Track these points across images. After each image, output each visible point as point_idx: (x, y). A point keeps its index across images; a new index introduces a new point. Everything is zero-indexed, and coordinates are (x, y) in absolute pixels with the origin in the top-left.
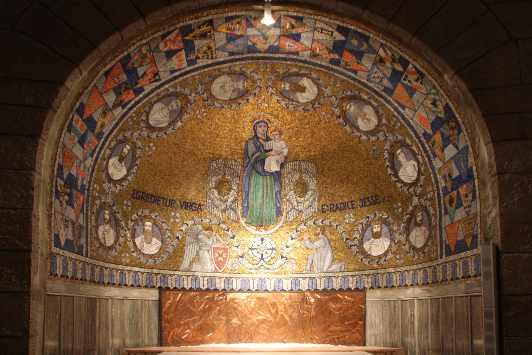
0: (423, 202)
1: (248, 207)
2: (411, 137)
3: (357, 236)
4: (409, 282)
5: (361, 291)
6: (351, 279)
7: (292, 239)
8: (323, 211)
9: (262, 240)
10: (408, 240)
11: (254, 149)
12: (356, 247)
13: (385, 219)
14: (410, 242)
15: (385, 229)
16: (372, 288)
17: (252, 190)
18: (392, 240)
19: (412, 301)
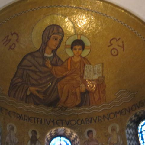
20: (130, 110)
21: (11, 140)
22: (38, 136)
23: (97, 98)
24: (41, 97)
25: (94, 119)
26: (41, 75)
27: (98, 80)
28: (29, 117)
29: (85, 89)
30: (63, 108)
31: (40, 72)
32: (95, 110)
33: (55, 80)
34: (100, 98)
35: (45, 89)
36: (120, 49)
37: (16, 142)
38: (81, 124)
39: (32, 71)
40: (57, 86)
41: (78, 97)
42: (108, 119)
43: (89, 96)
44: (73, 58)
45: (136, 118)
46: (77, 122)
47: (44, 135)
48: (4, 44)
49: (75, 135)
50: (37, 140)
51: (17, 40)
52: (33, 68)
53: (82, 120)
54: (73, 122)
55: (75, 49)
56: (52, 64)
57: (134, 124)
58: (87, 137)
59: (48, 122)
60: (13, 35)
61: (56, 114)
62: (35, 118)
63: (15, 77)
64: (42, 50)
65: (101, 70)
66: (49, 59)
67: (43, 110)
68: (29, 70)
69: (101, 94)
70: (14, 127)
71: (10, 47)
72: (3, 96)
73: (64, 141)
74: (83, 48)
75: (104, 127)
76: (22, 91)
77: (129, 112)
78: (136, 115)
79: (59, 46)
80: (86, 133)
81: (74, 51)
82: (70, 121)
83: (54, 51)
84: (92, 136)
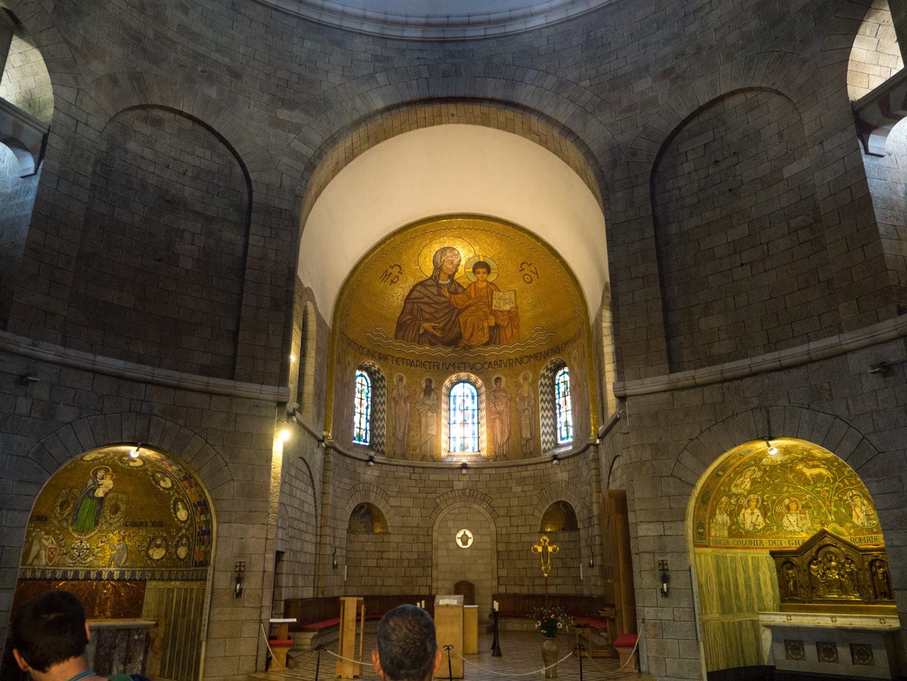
0: (187, 534)
1: (76, 519)
2: (186, 500)
3: (146, 544)
4: (173, 577)
5: (143, 581)
6: (137, 572)
7: (102, 542)
8: (126, 525)
9: (81, 542)
10: (176, 552)
11: (92, 483)
12: (143, 552)
13: (165, 537)
14: (177, 554)
15: (164, 543)
16: (150, 579)
17: (82, 508)
18: (167, 551)
19: (173, 589)
20: (545, 355)
21: (399, 395)
22: (433, 386)
23: (509, 335)
24: (438, 334)
26: (437, 307)
31: (436, 303)
32: (506, 351)
33: (457, 310)
34: (512, 335)
35: (443, 324)
36: (534, 276)
37: (406, 395)
39: (425, 303)
42: (521, 364)
45: (553, 365)
46: (483, 366)
47: (441, 383)
49: (480, 382)
50: (432, 390)
51: (399, 272)
52: (426, 300)
53: (490, 363)
54: (479, 366)
55: (479, 273)
56: (450, 293)
57: (551, 373)
59: (447, 366)
60: (395, 268)
61: (457, 356)
63: (402, 314)
65: (513, 299)
67: (441, 351)
68: (421, 302)
69: (514, 330)
71: (392, 282)
72: (389, 341)
73: (468, 388)
74: (489, 271)
75: (516, 375)
77: (545, 358)
78: (552, 362)
79: (456, 270)
80: (493, 380)
82: (474, 365)
83: (451, 277)
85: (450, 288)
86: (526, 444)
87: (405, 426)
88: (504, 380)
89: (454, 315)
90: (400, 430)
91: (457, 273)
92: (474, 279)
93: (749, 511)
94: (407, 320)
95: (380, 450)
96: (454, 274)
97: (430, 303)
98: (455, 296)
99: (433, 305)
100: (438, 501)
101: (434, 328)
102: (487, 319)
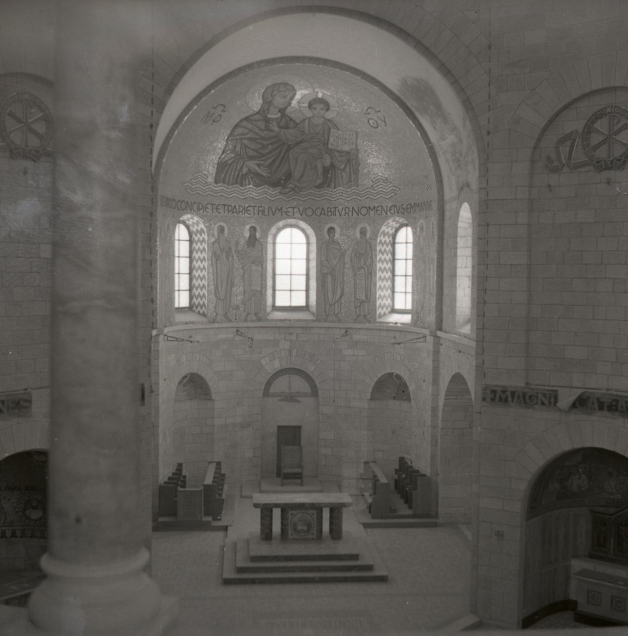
22: (258, 235)
25: (338, 210)
26: (262, 142)
27: (350, 153)
28: (246, 206)
29: (330, 163)
30: (297, 189)
33: (286, 147)
34: (350, 181)
38: (320, 216)
40: (288, 157)
41: (319, 173)
43: (335, 172)
44: (312, 119)
46: (314, 212)
48: (203, 123)
50: (256, 239)
51: (222, 111)
53: (323, 208)
56: (279, 126)
58: (327, 236)
59: (274, 210)
62: (254, 207)
64: (264, 111)
66: (274, 121)
70: (224, 228)
71: (214, 121)
76: (236, 169)
80: (326, 229)
81: (313, 111)
83: (282, 111)
84: (334, 236)
85: (280, 122)
86: (360, 306)
87: (227, 284)
88: (338, 230)
89: (284, 151)
90: (222, 287)
91: (289, 107)
92: (309, 114)
93: (577, 476)
94: (229, 160)
95: (201, 312)
96: (286, 108)
97: (256, 139)
98: (285, 130)
99: (259, 141)
100: (263, 362)
101: (259, 165)
102: (322, 158)
